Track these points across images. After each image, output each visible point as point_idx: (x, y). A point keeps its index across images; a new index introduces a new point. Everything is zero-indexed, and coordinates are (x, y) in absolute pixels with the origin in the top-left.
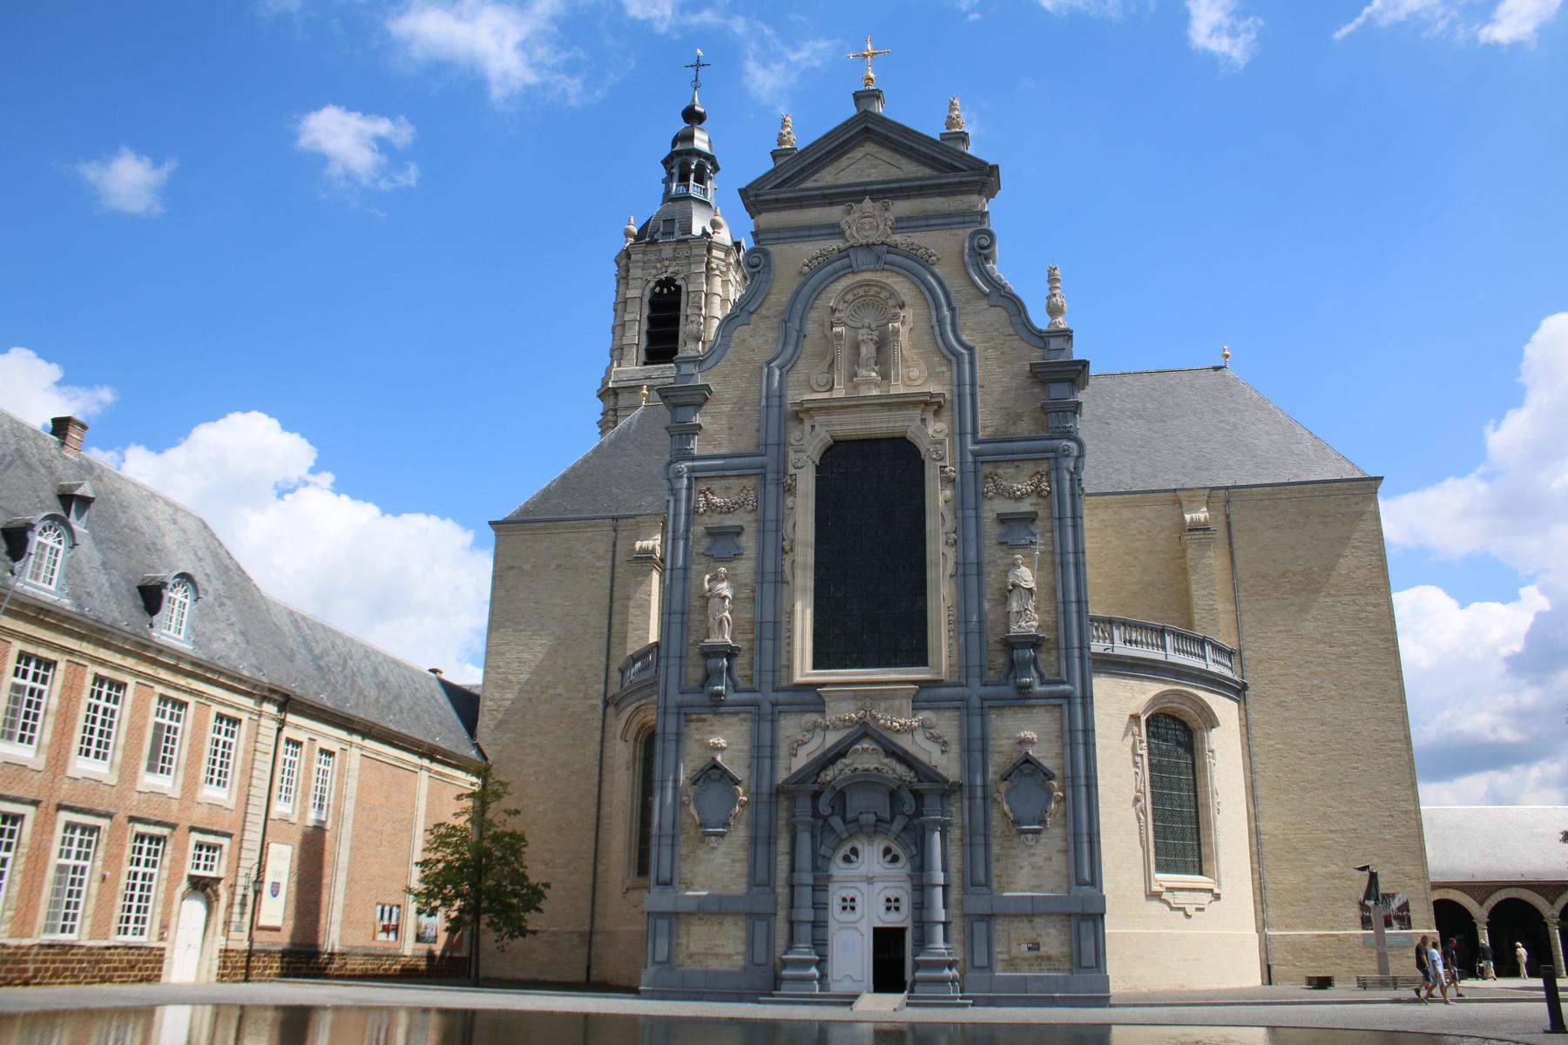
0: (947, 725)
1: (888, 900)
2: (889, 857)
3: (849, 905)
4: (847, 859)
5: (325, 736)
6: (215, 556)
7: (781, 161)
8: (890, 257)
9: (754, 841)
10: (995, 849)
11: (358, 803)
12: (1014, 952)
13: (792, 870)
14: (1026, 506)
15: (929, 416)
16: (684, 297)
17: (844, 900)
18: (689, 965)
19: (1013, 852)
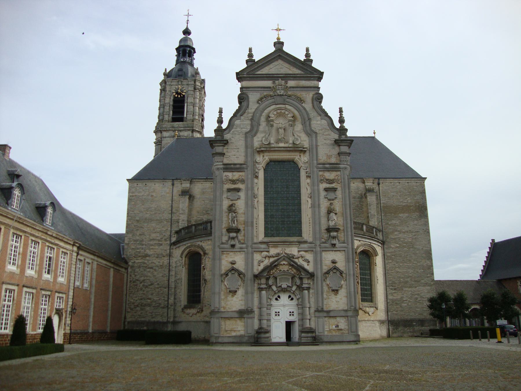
0: (309, 256)
1: (290, 312)
2: (290, 299)
3: (277, 314)
4: (276, 299)
5: (88, 258)
7: (250, 63)
8: (288, 100)
9: (246, 293)
10: (325, 296)
11: (96, 281)
12: (331, 328)
13: (260, 302)
15: (302, 155)
16: (186, 98)
17: (276, 312)
18: (226, 334)
19: (330, 297)
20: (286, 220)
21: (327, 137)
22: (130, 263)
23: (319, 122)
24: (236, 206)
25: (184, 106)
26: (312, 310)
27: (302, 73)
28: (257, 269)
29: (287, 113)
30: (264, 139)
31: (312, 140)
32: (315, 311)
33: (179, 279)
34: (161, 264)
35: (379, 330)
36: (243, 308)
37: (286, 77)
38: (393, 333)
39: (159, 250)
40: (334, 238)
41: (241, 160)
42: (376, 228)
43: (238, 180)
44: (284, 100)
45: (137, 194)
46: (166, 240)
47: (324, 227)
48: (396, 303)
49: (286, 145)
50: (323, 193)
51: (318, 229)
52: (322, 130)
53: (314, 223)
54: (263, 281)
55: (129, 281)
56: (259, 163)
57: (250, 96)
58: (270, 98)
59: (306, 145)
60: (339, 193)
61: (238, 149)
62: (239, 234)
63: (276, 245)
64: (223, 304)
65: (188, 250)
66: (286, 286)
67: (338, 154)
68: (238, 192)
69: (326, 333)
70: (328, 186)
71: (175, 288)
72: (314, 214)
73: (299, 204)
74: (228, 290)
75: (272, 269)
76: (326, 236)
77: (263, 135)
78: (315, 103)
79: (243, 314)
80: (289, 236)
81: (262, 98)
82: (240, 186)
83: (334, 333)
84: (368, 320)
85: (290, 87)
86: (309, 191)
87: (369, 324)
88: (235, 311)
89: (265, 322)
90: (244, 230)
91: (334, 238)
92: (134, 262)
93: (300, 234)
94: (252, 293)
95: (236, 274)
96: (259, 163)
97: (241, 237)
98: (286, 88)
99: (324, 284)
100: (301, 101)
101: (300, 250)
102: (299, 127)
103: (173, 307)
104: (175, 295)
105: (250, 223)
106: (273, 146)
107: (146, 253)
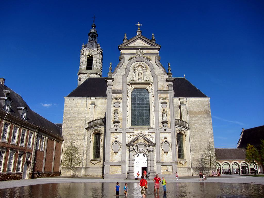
0: (154, 135)
3: (138, 163)
4: (137, 156)
6: (24, 103)
10: (161, 155)
12: (164, 171)
14: (165, 101)
15: (150, 86)
16: (93, 58)
20: (142, 117)
21: (163, 77)
22: (65, 138)
23: (158, 70)
24: (118, 110)
25: (92, 62)
26: (155, 162)
27: (151, 46)
28: (128, 141)
29: (143, 65)
30: (132, 78)
31: (155, 79)
32: (156, 162)
33: (89, 146)
34: (80, 138)
35: (187, 173)
36: (121, 160)
37: (143, 48)
38: (194, 174)
39: (79, 132)
40: (165, 126)
41: (121, 88)
42: (185, 122)
43: (119, 98)
44: (142, 60)
45: (69, 104)
46: (83, 127)
47: (161, 120)
48: (195, 159)
49: (143, 81)
50: (160, 105)
51: (158, 122)
52: (160, 74)
53: (156, 119)
54: (131, 147)
55: (63, 147)
56: (129, 90)
57: (125, 57)
58: (135, 58)
59: (152, 81)
60: (168, 104)
61: (119, 83)
62: (119, 124)
63: (137, 129)
64: (111, 158)
65: (94, 132)
66: (142, 150)
67: (168, 86)
68: (119, 103)
69: (161, 174)
70: (163, 101)
71: (87, 150)
72: (155, 114)
73: (149, 110)
74: (114, 151)
75: (135, 141)
76: (162, 125)
77: (131, 76)
78: (157, 60)
79: (121, 163)
80: (143, 125)
81: (131, 58)
82: (119, 100)
83: (166, 174)
84: (182, 168)
85: (145, 53)
86: (153, 104)
87: (182, 169)
88: (117, 162)
89: (131, 167)
90: (122, 122)
91: (165, 126)
92: (67, 138)
93: (149, 124)
94: (126, 153)
95: (118, 143)
96: (129, 90)
97: (120, 125)
98: (143, 54)
99: (161, 149)
100: (150, 60)
101: (149, 132)
102: (149, 72)
103: (85, 160)
104: (87, 154)
105: (124, 119)
106: (136, 81)
107: (73, 133)
